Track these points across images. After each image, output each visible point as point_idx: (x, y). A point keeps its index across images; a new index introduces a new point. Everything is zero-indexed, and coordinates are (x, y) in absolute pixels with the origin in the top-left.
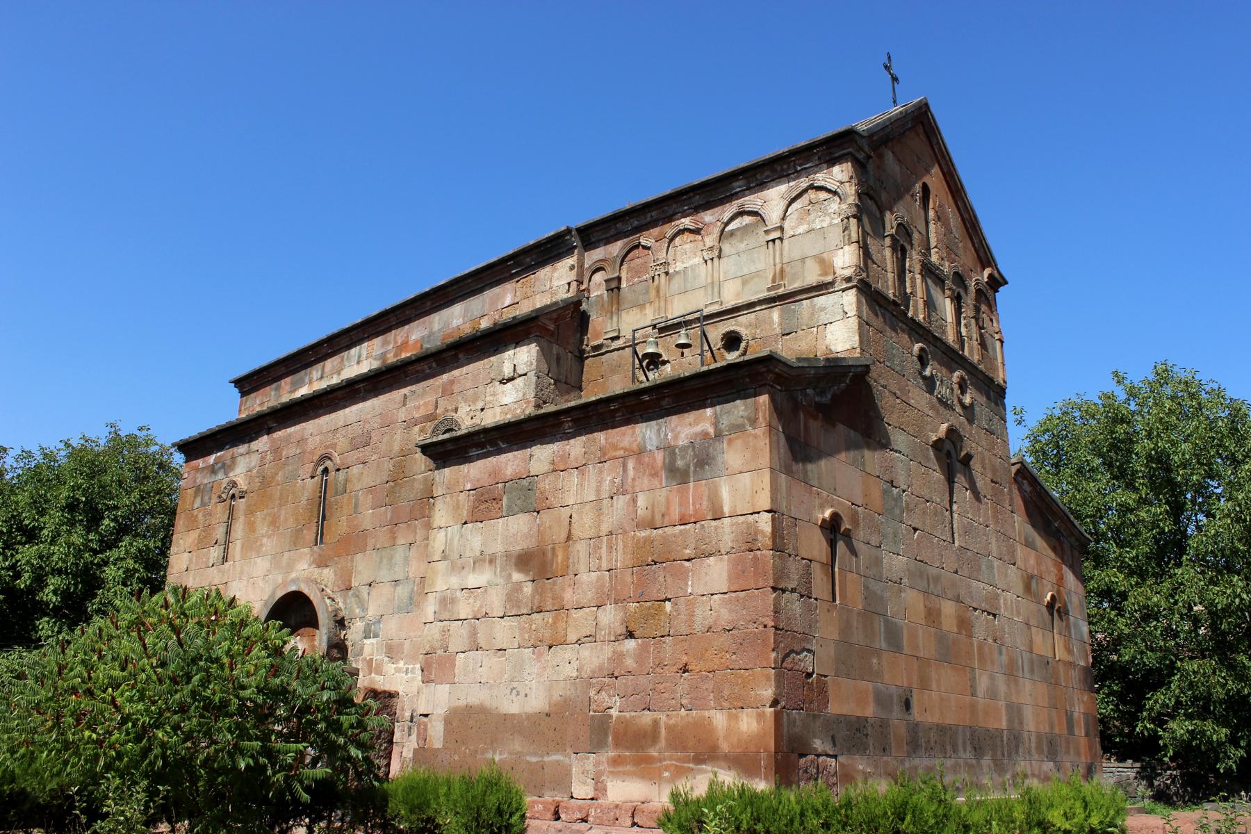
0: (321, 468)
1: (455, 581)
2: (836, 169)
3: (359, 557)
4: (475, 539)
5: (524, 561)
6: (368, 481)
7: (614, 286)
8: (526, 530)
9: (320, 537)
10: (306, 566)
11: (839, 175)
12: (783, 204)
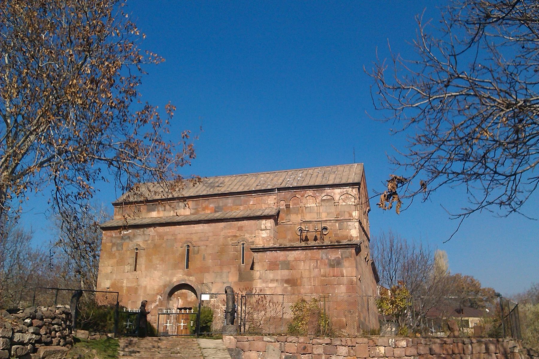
1: (264, 285)
2: (354, 190)
3: (206, 274)
4: (271, 275)
5: (287, 281)
6: (209, 251)
7: (288, 206)
8: (288, 274)
9: (187, 267)
11: (354, 191)
12: (339, 196)
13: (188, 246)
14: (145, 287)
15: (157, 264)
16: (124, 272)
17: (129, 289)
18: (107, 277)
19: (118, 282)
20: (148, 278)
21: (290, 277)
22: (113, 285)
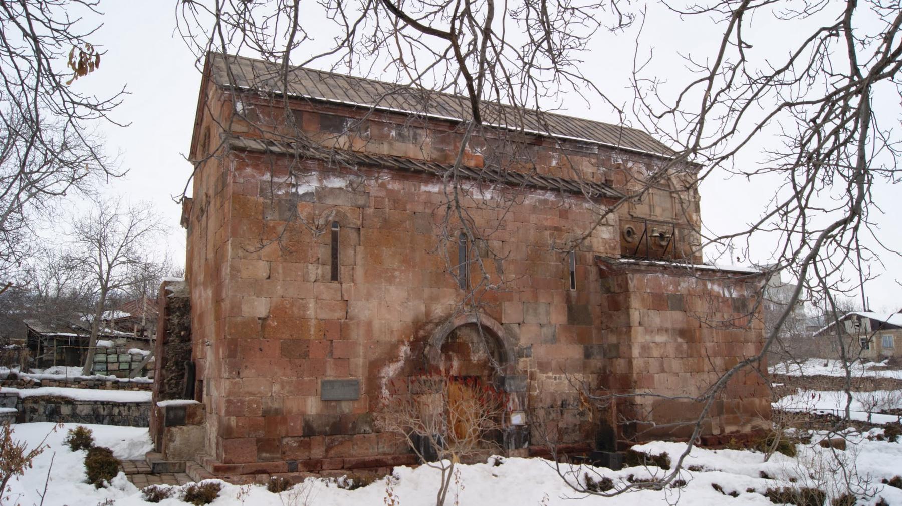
0: (457, 233)
1: (648, 338)
3: (507, 303)
4: (656, 318)
5: (682, 333)
10: (452, 302)
13: (464, 235)
14: (369, 324)
15: (394, 269)
16: (305, 280)
17: (325, 326)
18: (257, 287)
19: (292, 305)
20: (374, 303)
21: (685, 326)
22: (278, 311)
